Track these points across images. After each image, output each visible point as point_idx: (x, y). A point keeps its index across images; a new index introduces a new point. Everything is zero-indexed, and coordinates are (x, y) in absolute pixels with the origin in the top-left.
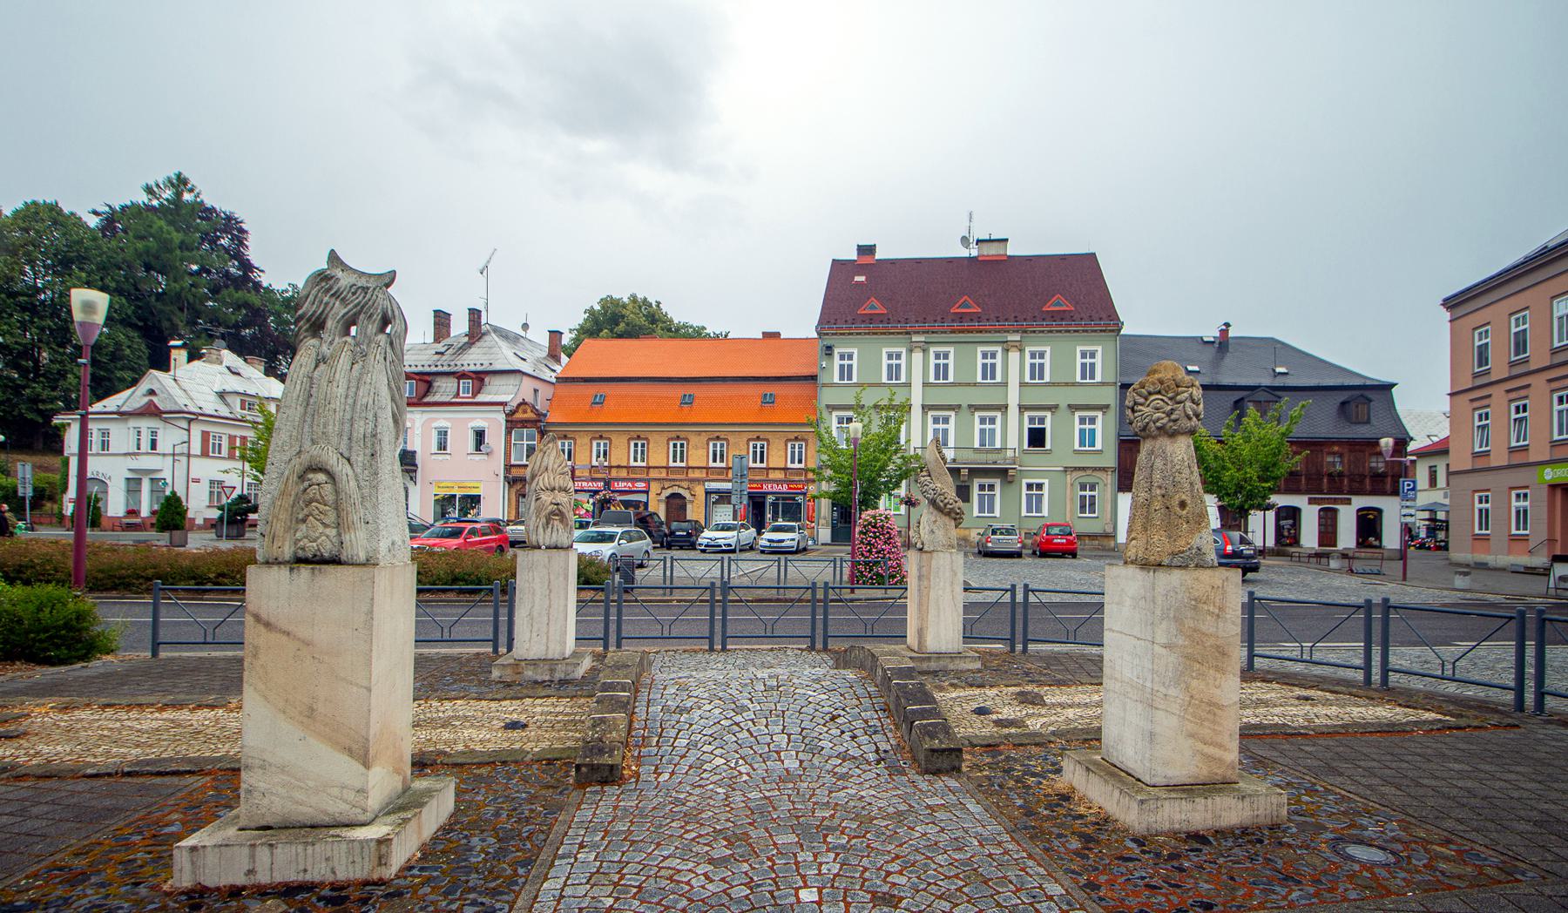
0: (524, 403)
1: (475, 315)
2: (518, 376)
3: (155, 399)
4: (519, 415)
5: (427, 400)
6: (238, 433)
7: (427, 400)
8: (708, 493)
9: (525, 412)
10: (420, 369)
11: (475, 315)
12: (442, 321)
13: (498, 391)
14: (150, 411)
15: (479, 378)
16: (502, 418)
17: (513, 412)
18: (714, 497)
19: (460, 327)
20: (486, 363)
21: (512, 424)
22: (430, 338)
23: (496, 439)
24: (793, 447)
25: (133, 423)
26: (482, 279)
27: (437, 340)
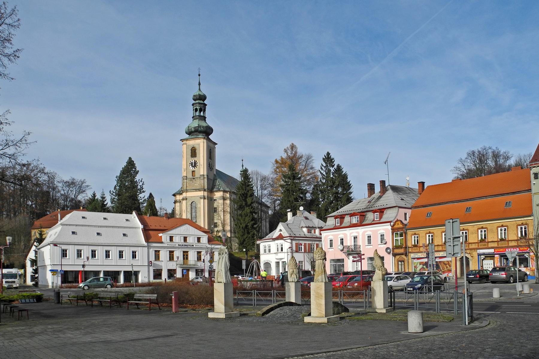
0: (397, 221)
1: (383, 183)
2: (397, 208)
3: (281, 232)
4: (396, 226)
5: (364, 223)
6: (307, 242)
7: (364, 223)
8: (479, 255)
9: (398, 225)
10: (361, 210)
11: (383, 183)
12: (371, 187)
13: (389, 215)
14: (280, 237)
15: (381, 211)
16: (390, 228)
17: (394, 225)
18: (483, 257)
19: (378, 189)
20: (385, 204)
21: (394, 230)
22: (367, 196)
23: (388, 238)
24: (522, 229)
25: (277, 242)
26: (385, 166)
27: (369, 196)
